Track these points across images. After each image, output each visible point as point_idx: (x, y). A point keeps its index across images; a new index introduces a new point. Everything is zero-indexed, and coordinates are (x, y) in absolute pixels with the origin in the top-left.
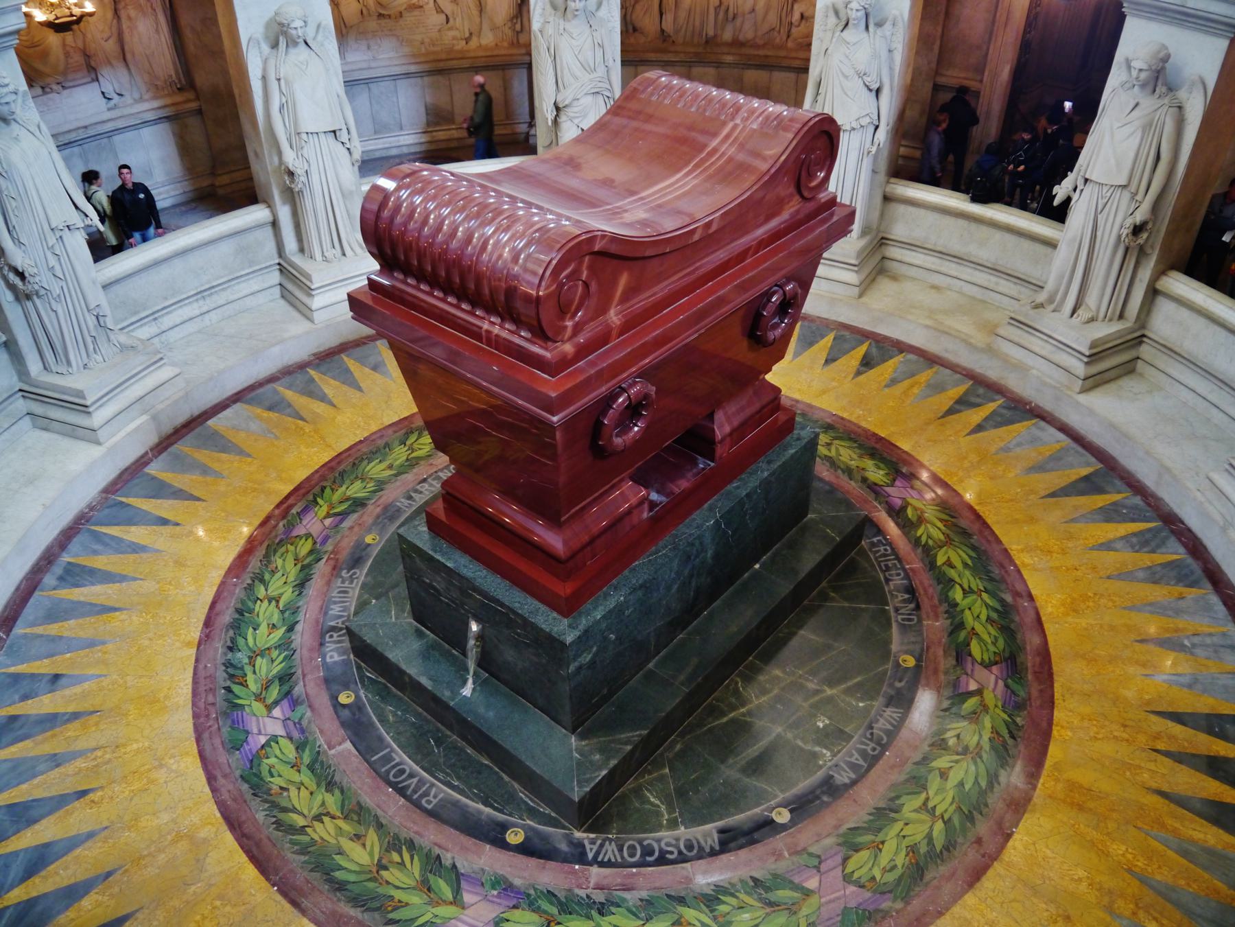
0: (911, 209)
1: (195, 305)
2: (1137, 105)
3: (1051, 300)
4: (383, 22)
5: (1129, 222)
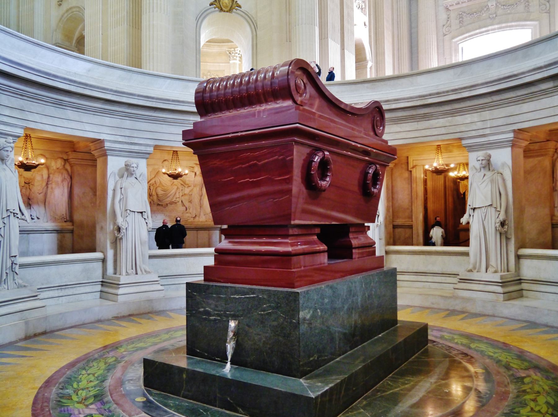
0: (398, 256)
1: (56, 291)
2: (485, 175)
3: (475, 268)
4: (159, 207)
5: (498, 220)
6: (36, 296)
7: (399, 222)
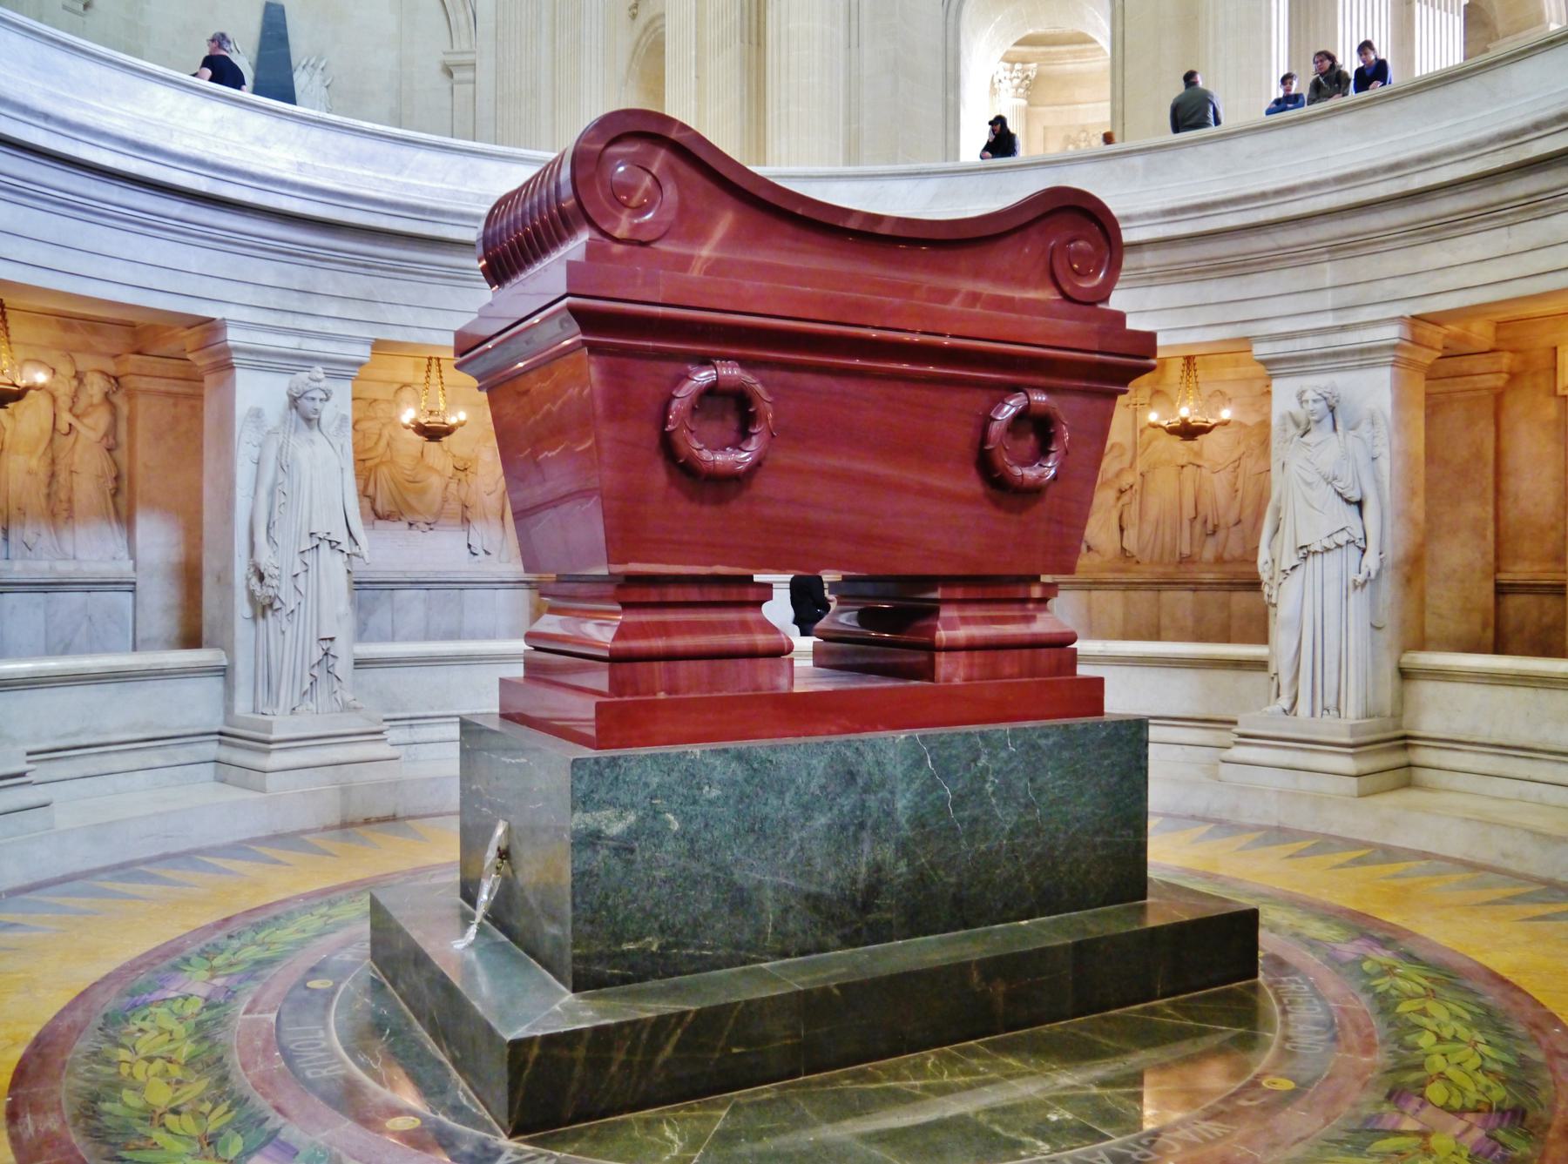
6: (380, 733)
7: (1519, 572)
